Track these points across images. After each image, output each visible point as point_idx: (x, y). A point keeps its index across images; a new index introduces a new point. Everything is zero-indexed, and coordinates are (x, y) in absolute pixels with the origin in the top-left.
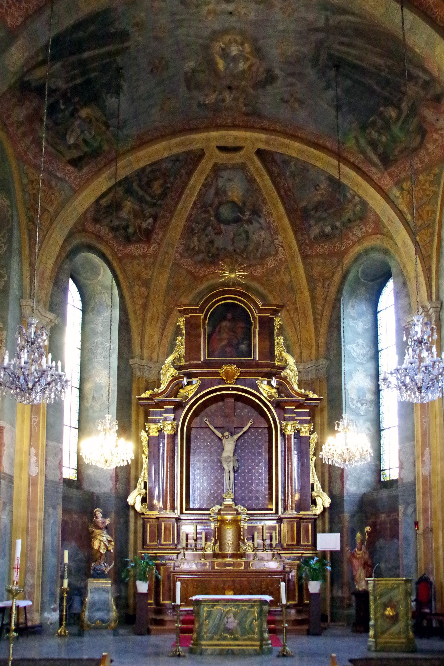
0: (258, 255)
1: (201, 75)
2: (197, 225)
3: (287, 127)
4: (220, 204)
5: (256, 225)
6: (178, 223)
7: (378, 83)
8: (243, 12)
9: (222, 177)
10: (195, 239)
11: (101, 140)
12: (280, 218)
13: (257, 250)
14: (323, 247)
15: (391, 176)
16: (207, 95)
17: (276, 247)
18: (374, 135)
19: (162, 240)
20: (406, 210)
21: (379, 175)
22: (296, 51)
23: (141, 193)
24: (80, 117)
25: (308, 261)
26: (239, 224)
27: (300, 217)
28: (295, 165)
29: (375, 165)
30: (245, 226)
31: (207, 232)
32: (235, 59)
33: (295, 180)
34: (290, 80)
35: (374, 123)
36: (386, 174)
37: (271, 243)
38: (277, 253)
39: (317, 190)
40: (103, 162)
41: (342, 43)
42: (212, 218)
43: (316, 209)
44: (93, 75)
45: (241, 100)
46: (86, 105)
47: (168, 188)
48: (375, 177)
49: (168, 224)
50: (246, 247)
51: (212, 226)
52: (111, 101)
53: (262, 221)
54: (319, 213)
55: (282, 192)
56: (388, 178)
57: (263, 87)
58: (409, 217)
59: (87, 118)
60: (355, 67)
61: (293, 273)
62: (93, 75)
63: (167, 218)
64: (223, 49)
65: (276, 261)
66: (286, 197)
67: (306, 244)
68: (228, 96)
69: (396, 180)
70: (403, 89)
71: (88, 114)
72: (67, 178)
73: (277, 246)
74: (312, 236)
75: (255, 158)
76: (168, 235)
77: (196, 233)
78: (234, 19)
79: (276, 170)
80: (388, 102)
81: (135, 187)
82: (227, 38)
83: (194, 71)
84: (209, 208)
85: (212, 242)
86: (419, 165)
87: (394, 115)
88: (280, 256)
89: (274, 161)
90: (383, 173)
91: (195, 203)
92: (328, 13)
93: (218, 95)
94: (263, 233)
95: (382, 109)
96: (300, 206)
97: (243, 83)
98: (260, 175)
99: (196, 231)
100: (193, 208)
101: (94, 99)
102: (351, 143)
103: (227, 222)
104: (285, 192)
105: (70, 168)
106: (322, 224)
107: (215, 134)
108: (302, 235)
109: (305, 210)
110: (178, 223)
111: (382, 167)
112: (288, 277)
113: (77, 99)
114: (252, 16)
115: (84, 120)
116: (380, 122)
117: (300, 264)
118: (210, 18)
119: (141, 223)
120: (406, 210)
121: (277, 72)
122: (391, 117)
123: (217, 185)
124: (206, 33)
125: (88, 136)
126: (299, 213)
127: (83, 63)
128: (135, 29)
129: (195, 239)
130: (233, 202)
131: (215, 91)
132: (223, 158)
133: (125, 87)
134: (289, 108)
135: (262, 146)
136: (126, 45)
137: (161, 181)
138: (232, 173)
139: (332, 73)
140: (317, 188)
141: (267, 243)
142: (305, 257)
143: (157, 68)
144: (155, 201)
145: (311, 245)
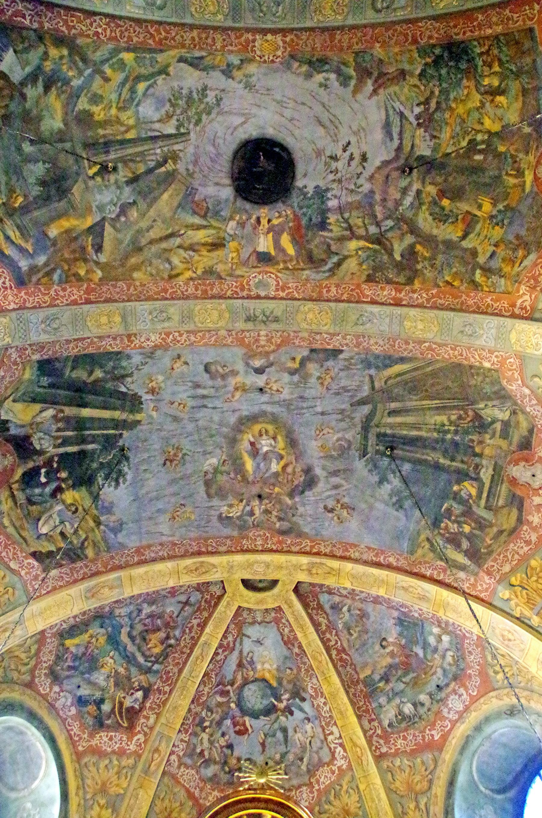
0: (304, 767)
1: (225, 478)
2: (209, 714)
3: (335, 546)
4: (246, 682)
5: (298, 715)
6: (181, 702)
7: (445, 453)
8: (275, 388)
9: (249, 637)
10: (205, 736)
11: (86, 539)
12: (334, 695)
13: (301, 759)
14: (405, 738)
15: (489, 573)
16: (231, 506)
17: (330, 749)
18: (454, 528)
19: (151, 728)
20: (527, 613)
21: (472, 580)
22: (338, 440)
23: (131, 648)
24: (63, 502)
25: (385, 764)
26: (273, 717)
27: (363, 693)
28: (349, 611)
29: (463, 568)
30: (282, 718)
31: (224, 728)
32: (265, 456)
33: (351, 635)
34: (335, 480)
35: (449, 511)
36: (482, 574)
37: (322, 742)
39: (384, 647)
40: (82, 572)
41: (393, 413)
42: (233, 705)
43: (386, 678)
44: (90, 447)
45: (275, 513)
46: (74, 487)
47: (170, 646)
48: (466, 587)
49: (165, 703)
50: (283, 755)
51: (233, 718)
52: (109, 492)
53: (306, 706)
54: (391, 685)
55: (334, 653)
56: (486, 578)
57: (303, 492)
58: (535, 621)
59: (73, 504)
60: (412, 442)
61: (362, 787)
62: (90, 447)
63: (165, 693)
64: (252, 444)
65: (333, 772)
66: (341, 661)
67: (378, 736)
68: (258, 508)
69: (498, 578)
70: (477, 450)
71: (75, 500)
72: (23, 573)
73: (332, 746)
74: (386, 723)
75: (293, 597)
76: (163, 720)
77: (206, 727)
78: (265, 398)
79: (323, 621)
80: (462, 476)
81: (124, 638)
82: (257, 428)
83: (216, 471)
84: (229, 688)
85: (230, 746)
86: (526, 549)
87: (474, 492)
88: (340, 762)
89: (320, 607)
90: (476, 574)
91: (206, 674)
92: (372, 372)
93: (245, 507)
94: (308, 727)
95: (455, 488)
96: (362, 676)
97: (277, 489)
98: (302, 627)
99: (207, 724)
100: (202, 682)
101: (85, 481)
102: (423, 551)
103: (255, 715)
104: (339, 652)
105: (32, 561)
106: (397, 701)
107: (239, 558)
108: (370, 721)
109: (368, 682)
110: (181, 702)
111: (473, 567)
112: (355, 797)
113: (64, 475)
114: (286, 395)
115: (68, 507)
116: (457, 509)
117: (373, 769)
118: (238, 395)
119: (124, 698)
120: (527, 613)
121: (318, 471)
122: (470, 495)
123: (241, 652)
124: (233, 419)
125: (69, 529)
126: (361, 686)
127: (80, 424)
128: (149, 397)
129: (205, 736)
130: (264, 680)
131: (241, 501)
132: (250, 599)
133: (129, 477)
134: (336, 518)
135: (303, 577)
136: (138, 417)
137: (162, 635)
138: (262, 630)
139: (386, 461)
140: (384, 643)
141: (317, 743)
142: (379, 758)
143: (171, 461)
144: (150, 664)
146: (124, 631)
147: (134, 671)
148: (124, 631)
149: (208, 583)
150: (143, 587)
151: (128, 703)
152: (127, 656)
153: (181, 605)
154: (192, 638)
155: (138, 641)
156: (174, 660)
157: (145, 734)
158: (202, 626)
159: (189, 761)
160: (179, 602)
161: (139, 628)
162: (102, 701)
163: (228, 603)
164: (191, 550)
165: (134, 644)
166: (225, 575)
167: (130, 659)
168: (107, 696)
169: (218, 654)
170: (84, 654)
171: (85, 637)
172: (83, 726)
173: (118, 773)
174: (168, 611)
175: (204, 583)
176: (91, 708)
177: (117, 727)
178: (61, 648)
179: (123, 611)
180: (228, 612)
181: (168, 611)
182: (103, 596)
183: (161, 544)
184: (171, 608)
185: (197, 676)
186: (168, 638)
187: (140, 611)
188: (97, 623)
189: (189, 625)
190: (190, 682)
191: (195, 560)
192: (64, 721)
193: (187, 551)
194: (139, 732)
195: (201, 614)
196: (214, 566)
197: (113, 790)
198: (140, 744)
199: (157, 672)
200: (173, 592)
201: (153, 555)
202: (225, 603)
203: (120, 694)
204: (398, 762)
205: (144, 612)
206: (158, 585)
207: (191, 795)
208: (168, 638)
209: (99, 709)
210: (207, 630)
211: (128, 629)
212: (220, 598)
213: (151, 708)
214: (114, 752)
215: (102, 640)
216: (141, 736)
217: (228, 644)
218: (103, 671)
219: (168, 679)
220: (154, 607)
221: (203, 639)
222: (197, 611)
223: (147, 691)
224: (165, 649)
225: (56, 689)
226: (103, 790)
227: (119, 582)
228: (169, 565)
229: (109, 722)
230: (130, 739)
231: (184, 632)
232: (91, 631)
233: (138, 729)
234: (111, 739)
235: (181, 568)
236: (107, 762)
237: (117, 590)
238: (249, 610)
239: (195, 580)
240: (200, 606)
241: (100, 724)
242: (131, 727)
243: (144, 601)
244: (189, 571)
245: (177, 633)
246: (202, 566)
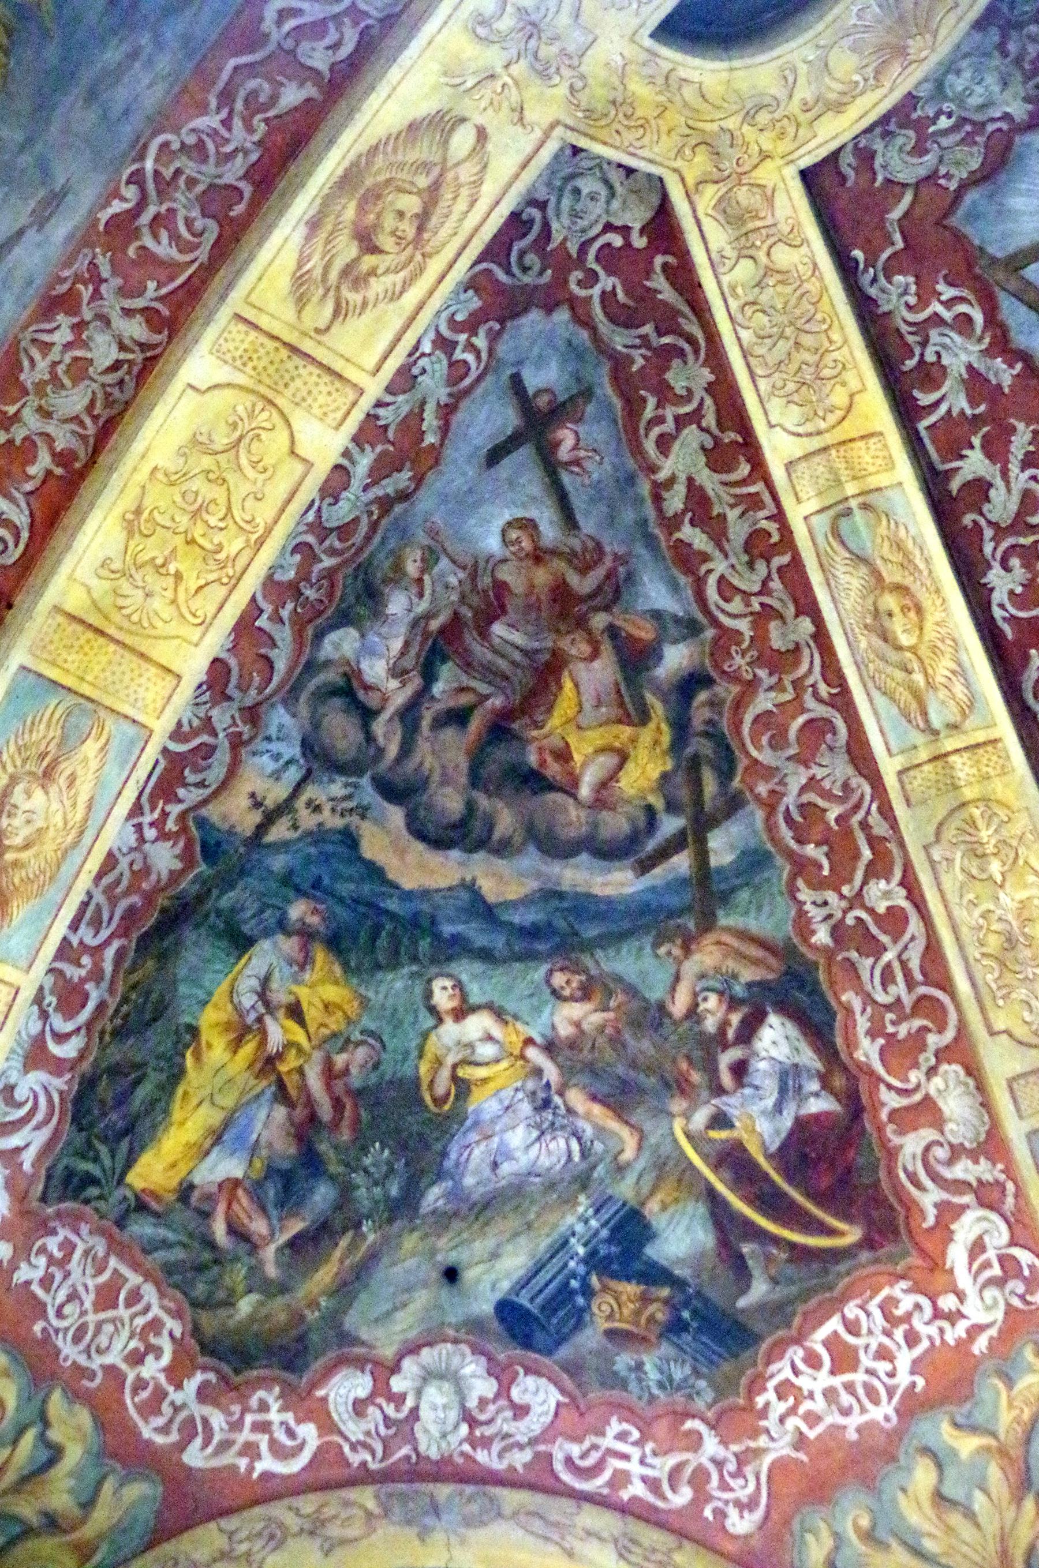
19: (992, 1145)
23: (504, 881)
47: (692, 683)
76: (1000, 1062)
81: (421, 871)
119: (720, 1121)
137: (593, 675)
144: (682, 863)
146: (386, 841)
147: (636, 963)
148: (386, 841)
149: (516, 224)
150: (205, 605)
151: (760, 1124)
152: (533, 932)
153: (525, 453)
154: (758, 548)
155: (506, 821)
156: (778, 743)
157: (987, 1196)
158: (736, 443)
160: (495, 456)
161: (444, 757)
162: (630, 1230)
163: (732, 216)
164: (233, 173)
165: (503, 849)
166: (548, 104)
167: (558, 934)
168: (625, 1189)
169: (980, 488)
170: (306, 1129)
171: (217, 1067)
172: (662, 1421)
174: (493, 544)
175: (498, 249)
176: (615, 1303)
177: (819, 1277)
178: (143, 1228)
179: (264, 776)
180: (784, 257)
181: (493, 544)
182: (48, 848)
183: (53, 304)
184: (492, 519)
185: (971, 705)
186: (635, 658)
187: (350, 692)
188: (196, 949)
189: (675, 501)
190: (962, 767)
191: (303, 204)
192: (540, 1480)
193: (216, 199)
194: (948, 1213)
195: (665, 394)
196: (441, 124)
198: (1009, 1266)
199: (754, 862)
200: (398, 446)
201: (74, 400)
202: (718, 237)
203: (685, 1125)
205: (375, 670)
206: (264, 513)
208: (635, 658)
209: (655, 1275)
210: (777, 447)
211: (396, 815)
212: (664, 228)
213: (902, 1052)
214: (912, 1406)
215: (323, 989)
216: (967, 1228)
217: (975, 382)
218: (484, 1104)
219: (840, 844)
220: (397, 604)
221: (802, 510)
222: (633, 407)
223: (796, 990)
224: (681, 728)
225: (347, 1387)
227: (55, 706)
228: (205, 364)
229: (759, 1290)
231: (687, 560)
232: (210, 1019)
233: (929, 1199)
234: (843, 1359)
235: (277, 311)
236: (923, 1477)
237: (91, 748)
238: (901, 116)
239: (431, 286)
240: (619, 364)
241: (720, 1336)
242: (887, 1224)
243: (314, 624)
244: (339, 289)
245: (657, 593)
246: (374, 195)
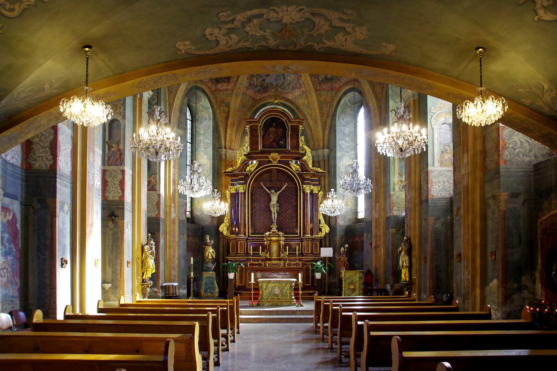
0: (290, 87)
10: (255, 79)
25: (318, 92)
38: (301, 87)
61: (310, 99)
85: (264, 80)
117: (314, 94)
129: (255, 79)
142: (316, 90)
145: (320, 84)
159: (250, 88)
173: (227, 96)
192: (205, 83)
197: (226, 101)
204: (323, 92)
207: (251, 97)
214: (224, 90)
226: (223, 101)
230: (229, 85)
